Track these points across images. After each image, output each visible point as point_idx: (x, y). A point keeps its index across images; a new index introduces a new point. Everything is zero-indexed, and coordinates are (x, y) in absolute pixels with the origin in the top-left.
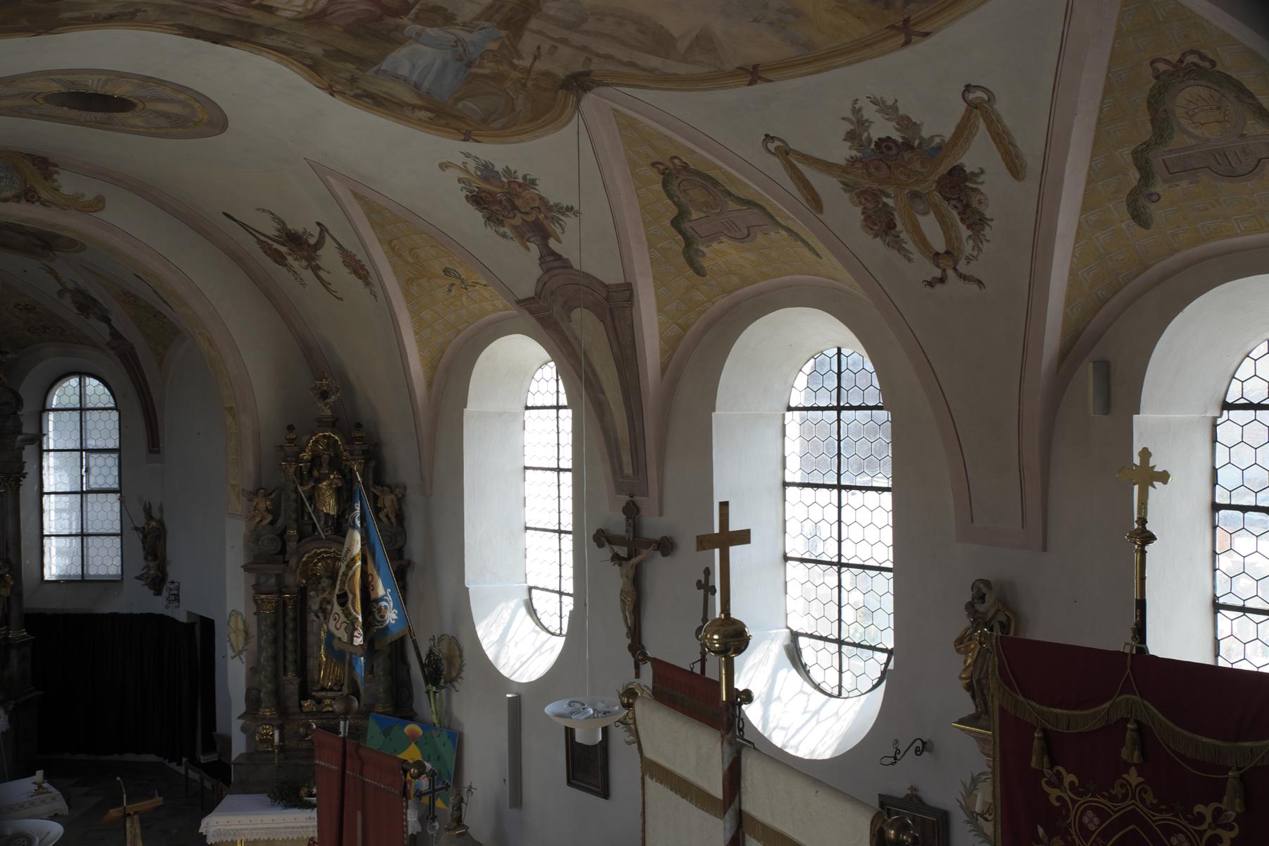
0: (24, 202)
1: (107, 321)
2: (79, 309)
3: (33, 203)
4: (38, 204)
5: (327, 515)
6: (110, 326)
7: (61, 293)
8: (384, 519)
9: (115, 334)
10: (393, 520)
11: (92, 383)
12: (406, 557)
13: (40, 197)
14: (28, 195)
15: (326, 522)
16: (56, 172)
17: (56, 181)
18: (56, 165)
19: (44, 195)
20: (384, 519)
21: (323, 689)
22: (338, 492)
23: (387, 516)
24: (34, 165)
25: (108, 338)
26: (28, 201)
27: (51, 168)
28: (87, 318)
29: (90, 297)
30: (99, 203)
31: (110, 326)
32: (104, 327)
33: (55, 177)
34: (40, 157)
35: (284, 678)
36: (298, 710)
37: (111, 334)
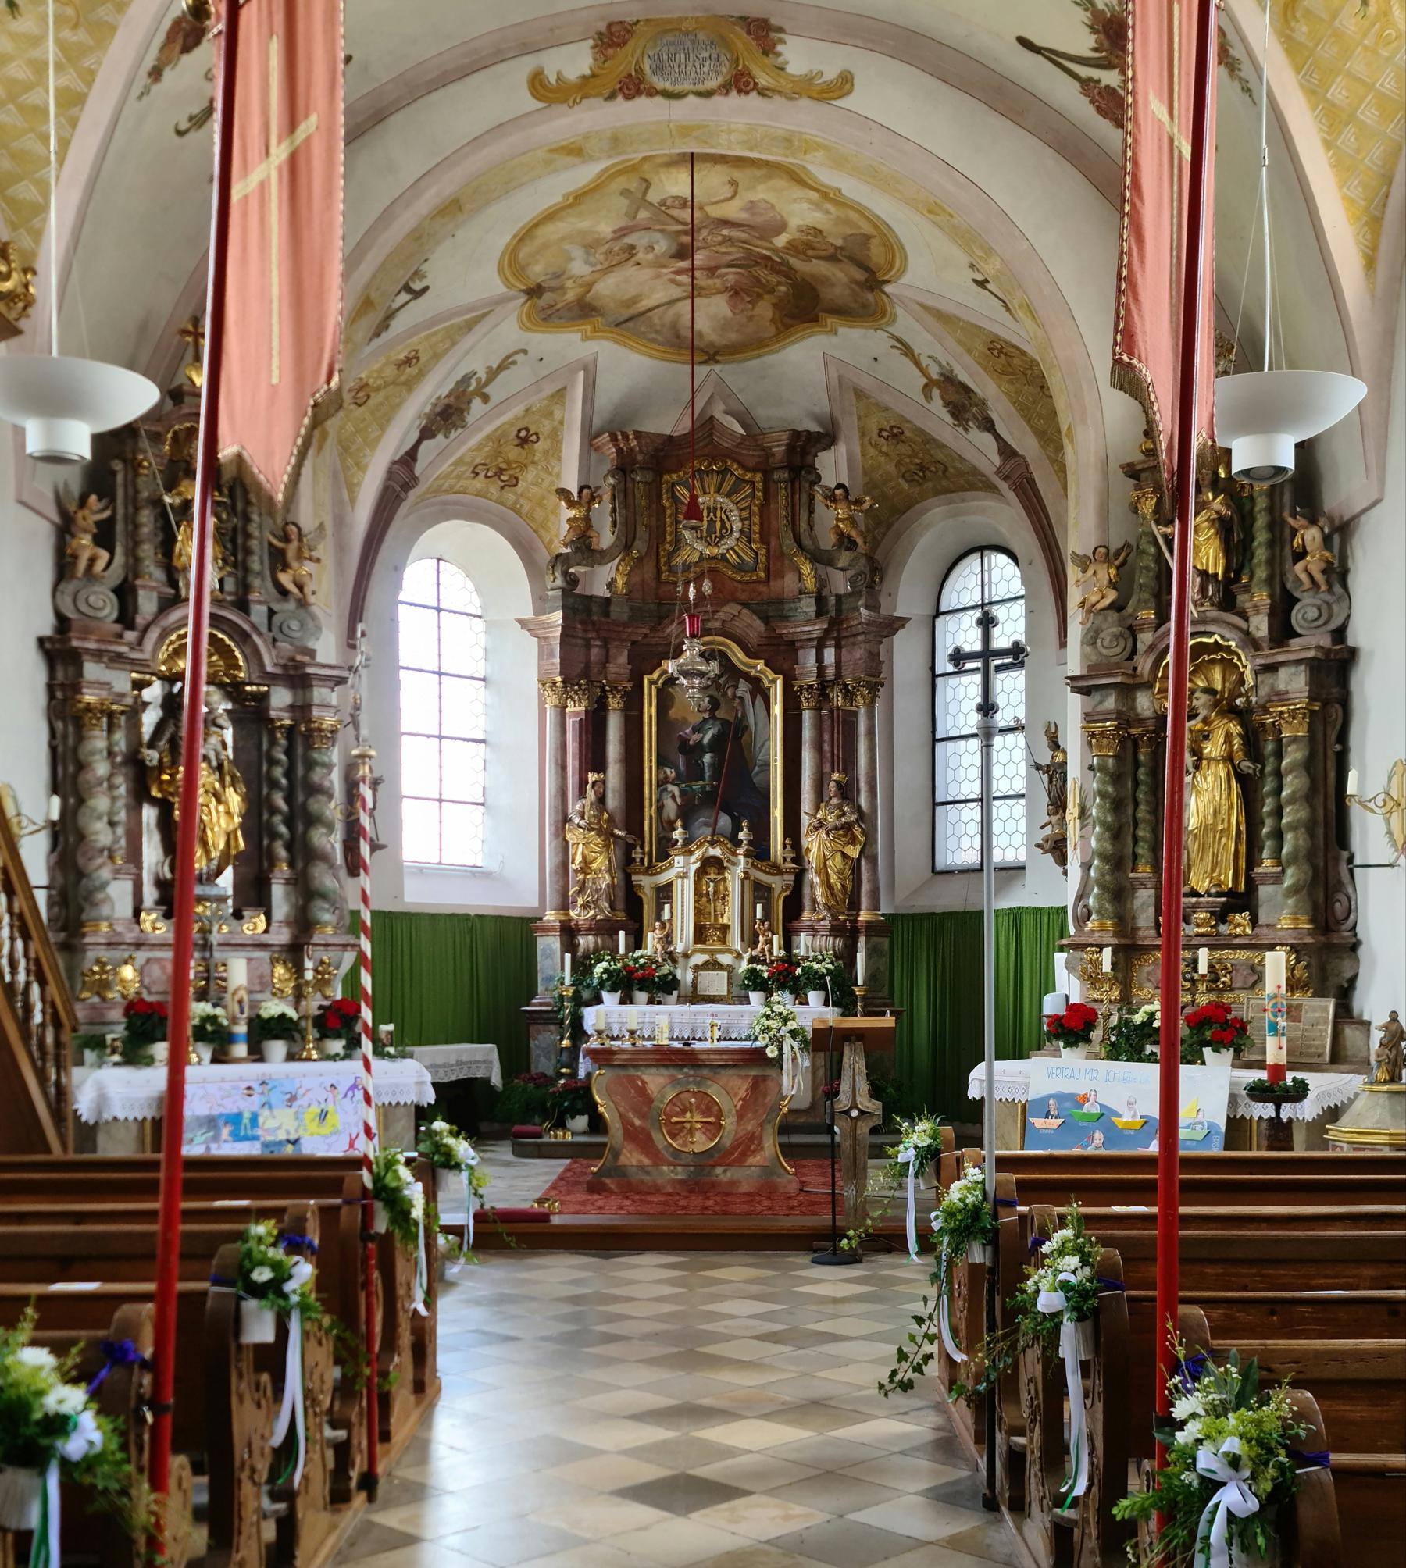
0: (734, 93)
1: (988, 426)
2: (954, 415)
3: (747, 93)
4: (754, 94)
5: (1203, 574)
6: (998, 437)
7: (927, 389)
8: (1303, 577)
9: (1006, 451)
10: (1319, 577)
11: (1001, 559)
12: (1351, 642)
13: (756, 84)
14: (740, 83)
15: (1203, 590)
16: (782, 41)
17: (779, 55)
18: (781, 30)
19: (763, 80)
20: (1303, 577)
21: (1194, 893)
22: (1224, 528)
23: (1306, 570)
24: (749, 33)
25: (997, 460)
26: (740, 91)
27: (772, 35)
28: (966, 430)
29: (960, 383)
30: (844, 84)
31: (998, 437)
32: (988, 438)
33: (779, 48)
34: (758, 20)
35: (1131, 875)
36: (1153, 932)
37: (1001, 453)
